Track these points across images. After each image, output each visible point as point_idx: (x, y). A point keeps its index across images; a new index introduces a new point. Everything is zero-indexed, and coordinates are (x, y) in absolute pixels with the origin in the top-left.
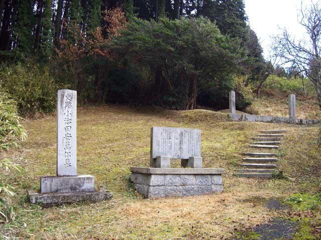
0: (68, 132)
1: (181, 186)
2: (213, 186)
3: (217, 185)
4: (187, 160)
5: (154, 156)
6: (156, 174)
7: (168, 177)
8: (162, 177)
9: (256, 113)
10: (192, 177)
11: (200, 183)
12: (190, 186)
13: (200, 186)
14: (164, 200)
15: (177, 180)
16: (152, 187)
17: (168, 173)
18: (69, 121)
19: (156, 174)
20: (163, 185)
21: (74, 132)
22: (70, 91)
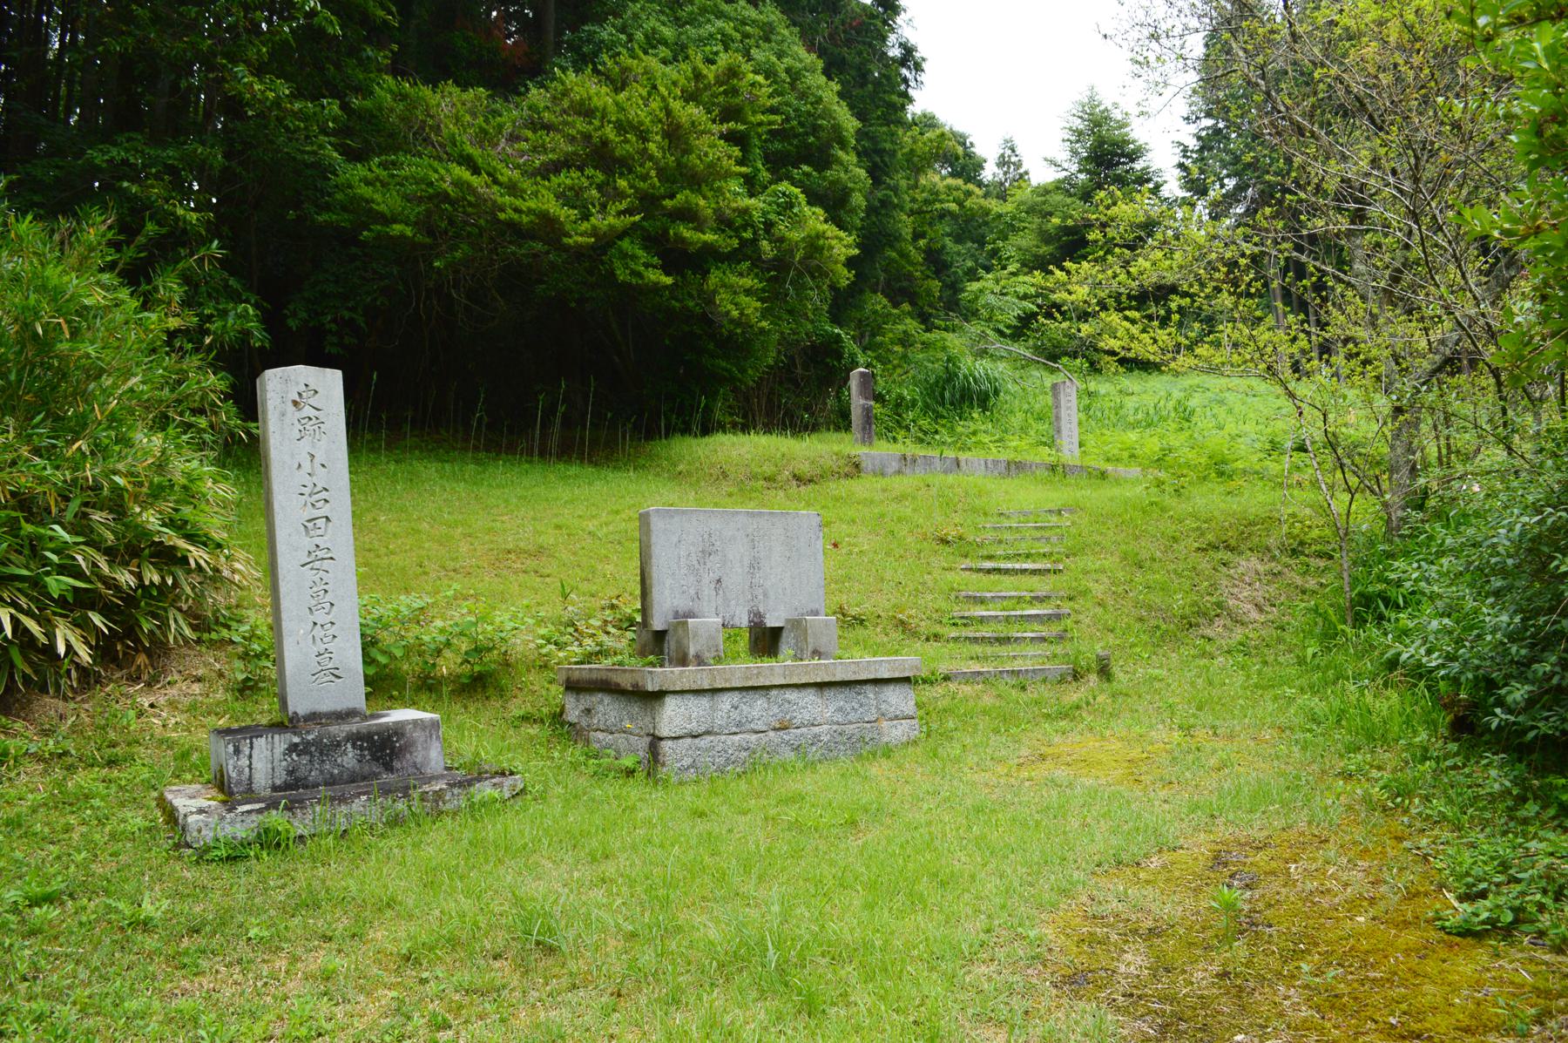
0: (317, 541)
1: (775, 729)
2: (885, 724)
3: (897, 718)
4: (776, 633)
5: (657, 624)
6: (682, 692)
7: (726, 702)
8: (704, 701)
9: (1413, 600)
10: (810, 696)
11: (839, 717)
12: (804, 730)
13: (839, 728)
14: (1039, 765)
15: (757, 709)
16: (670, 743)
17: (723, 686)
18: (317, 494)
19: (682, 692)
20: (708, 733)
21: (340, 537)
22: (302, 374)
